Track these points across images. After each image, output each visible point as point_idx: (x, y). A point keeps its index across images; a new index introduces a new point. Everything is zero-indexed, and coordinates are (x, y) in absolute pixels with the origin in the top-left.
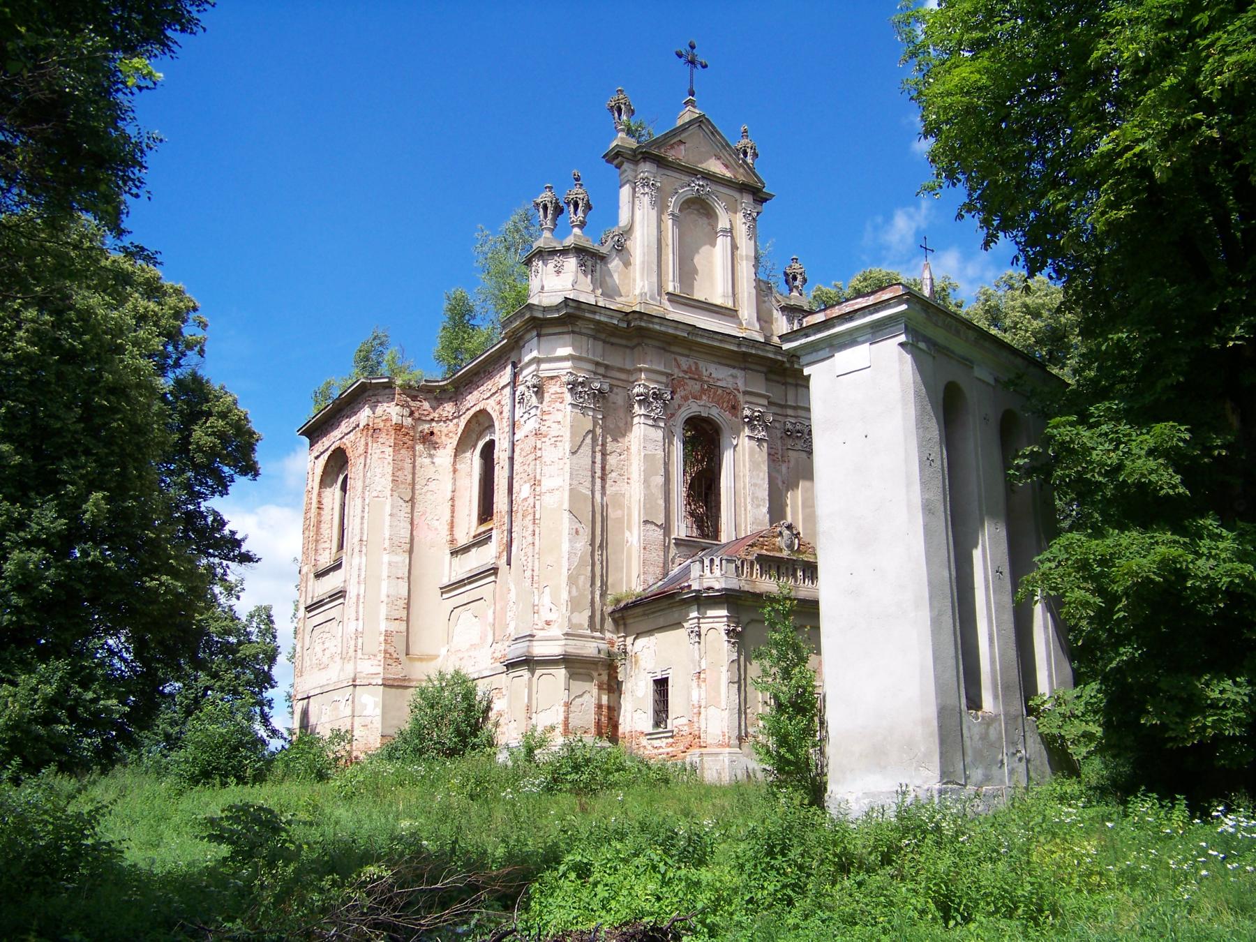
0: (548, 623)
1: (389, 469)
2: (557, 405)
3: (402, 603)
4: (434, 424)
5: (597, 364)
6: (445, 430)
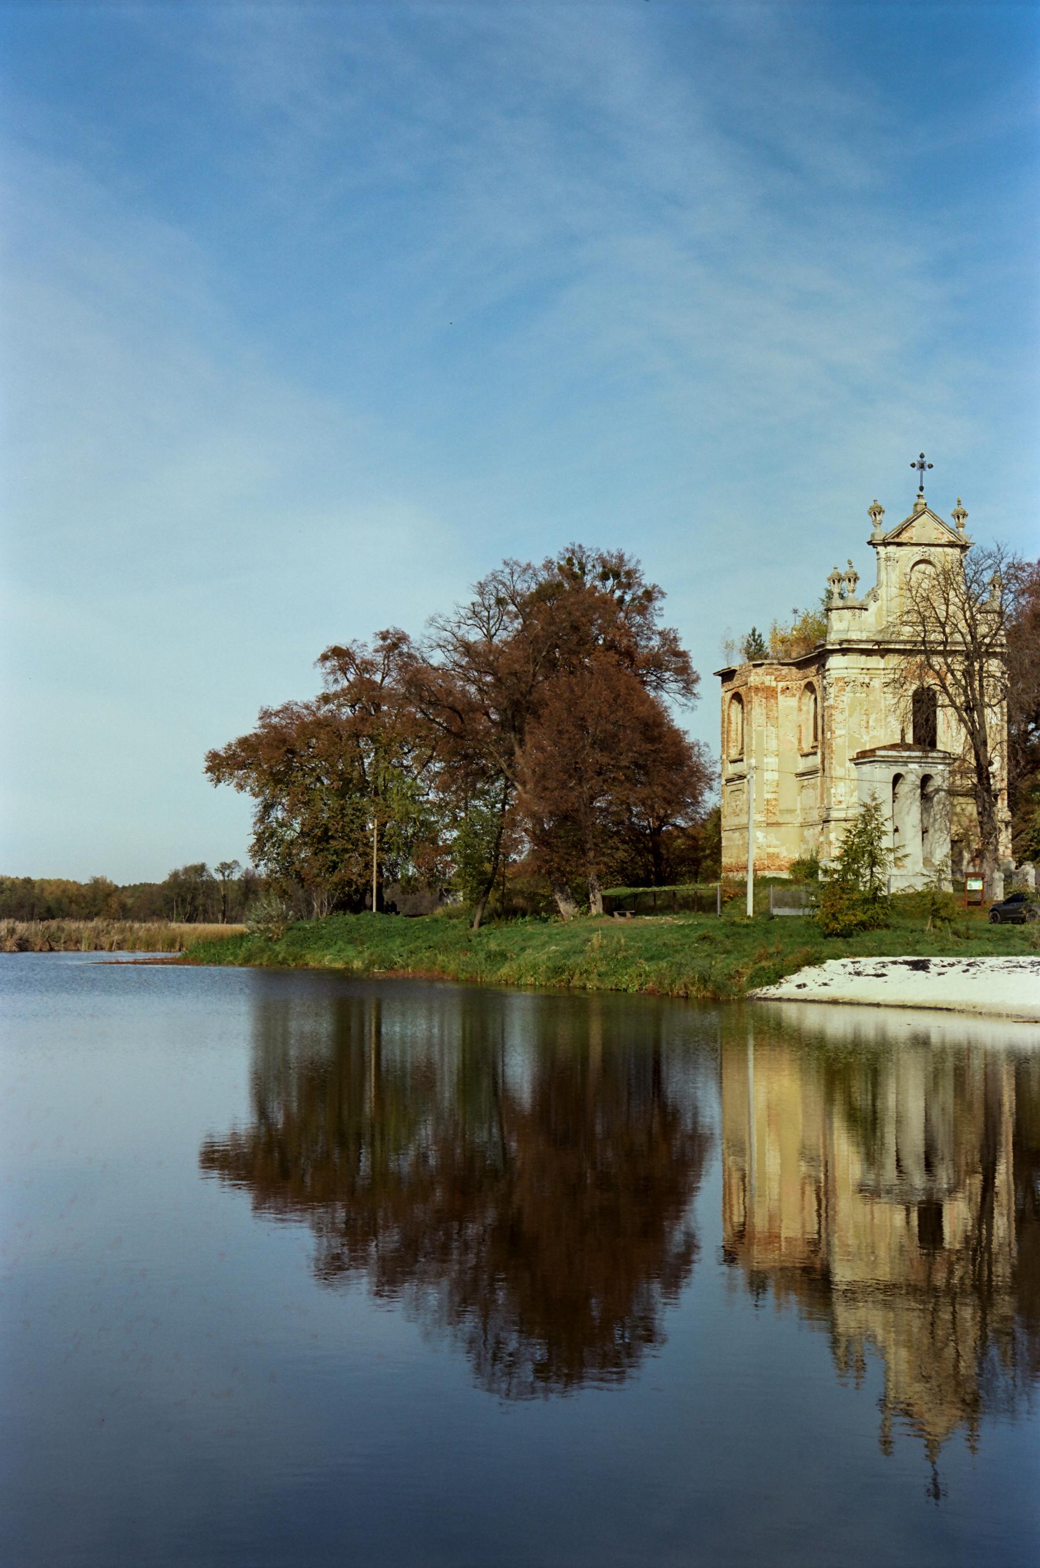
0: (840, 802)
1: (764, 711)
2: (842, 693)
3: (775, 784)
4: (788, 683)
5: (863, 669)
6: (795, 687)
